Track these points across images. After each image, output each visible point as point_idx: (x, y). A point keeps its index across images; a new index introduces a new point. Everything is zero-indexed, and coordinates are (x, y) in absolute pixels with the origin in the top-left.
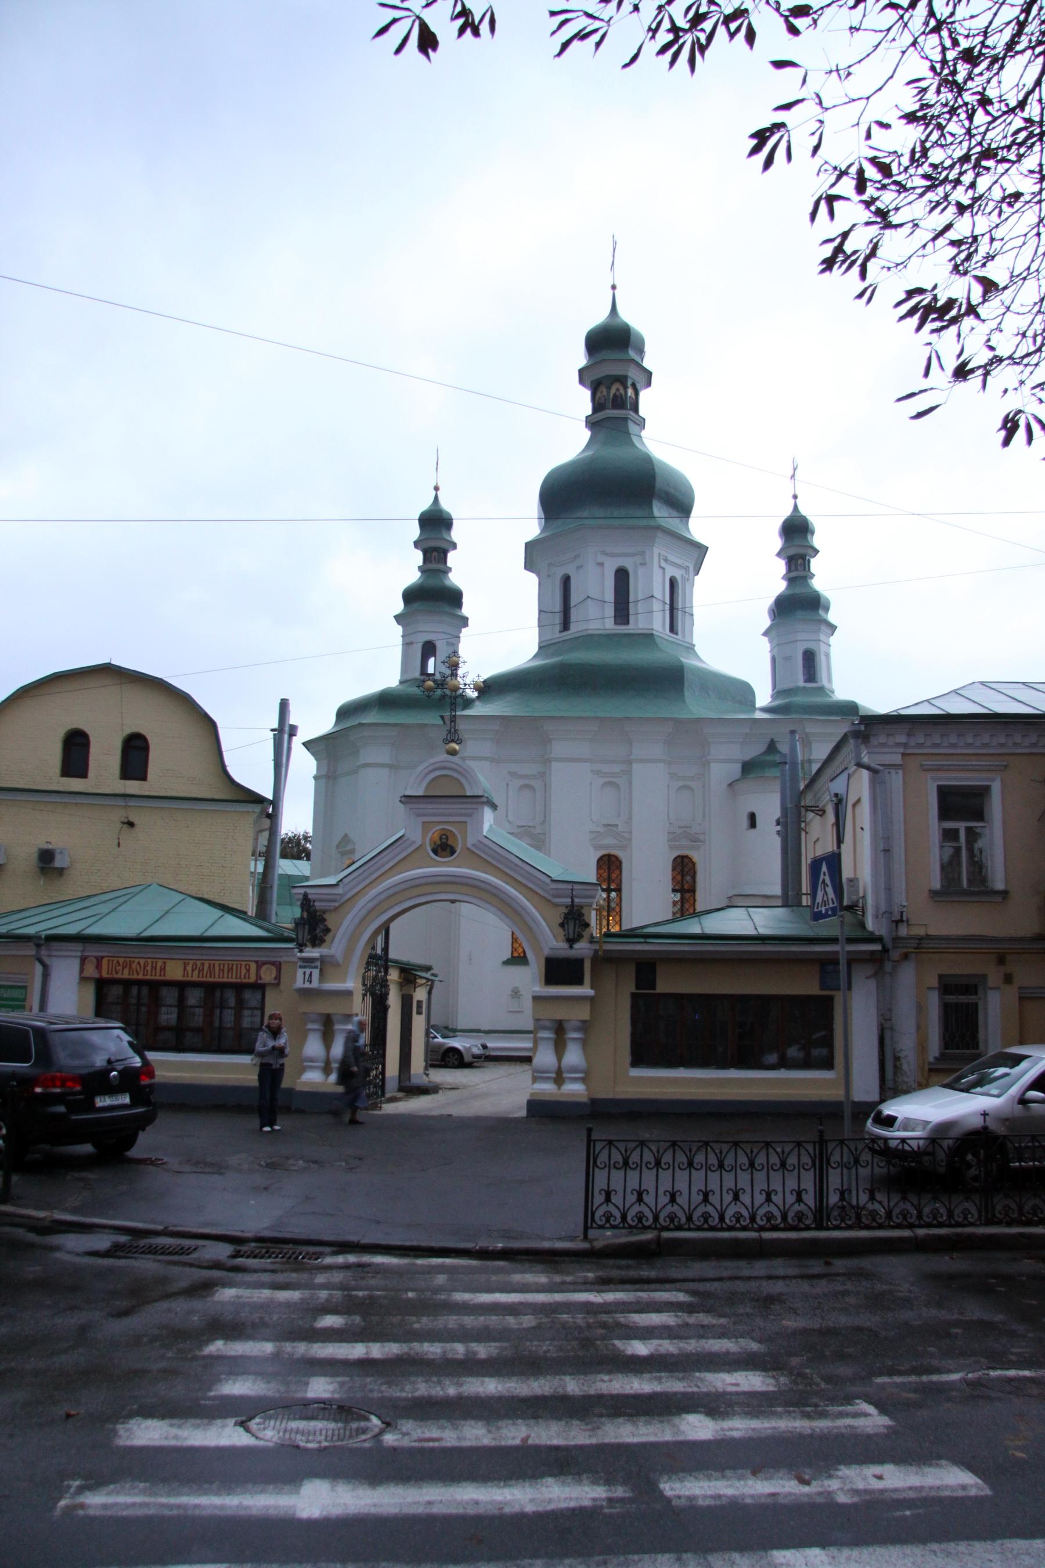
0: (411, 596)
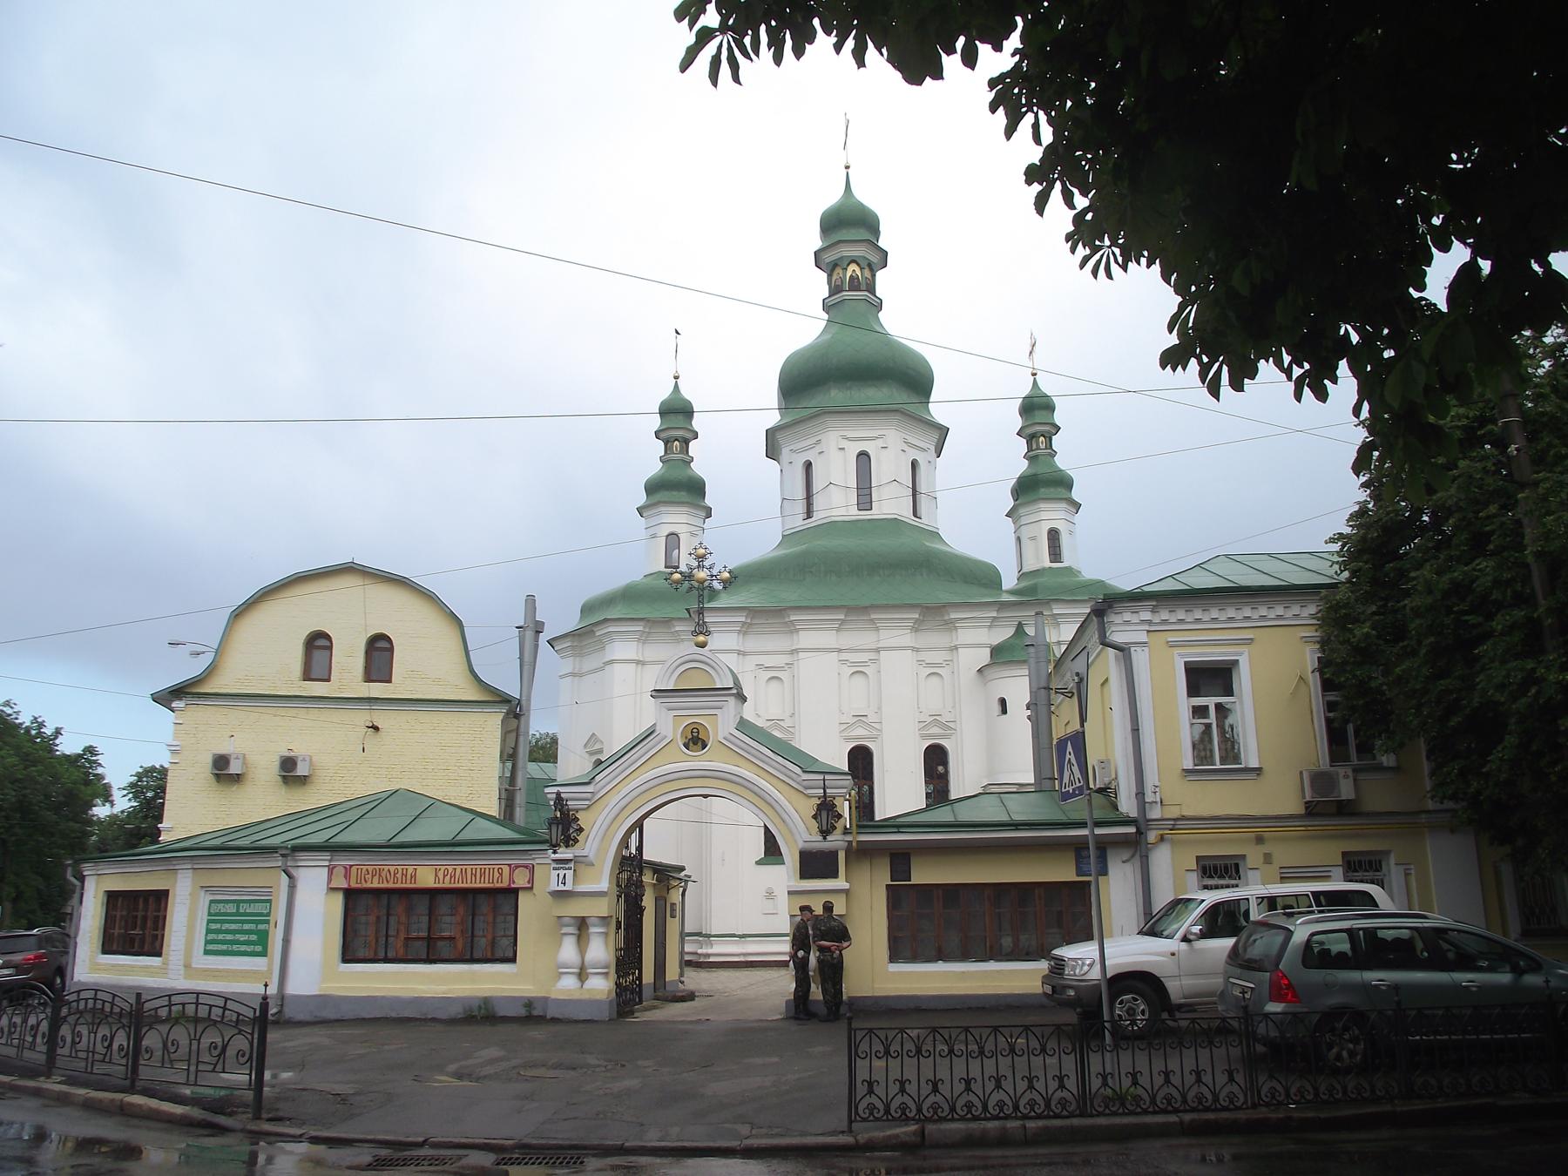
0: (653, 487)
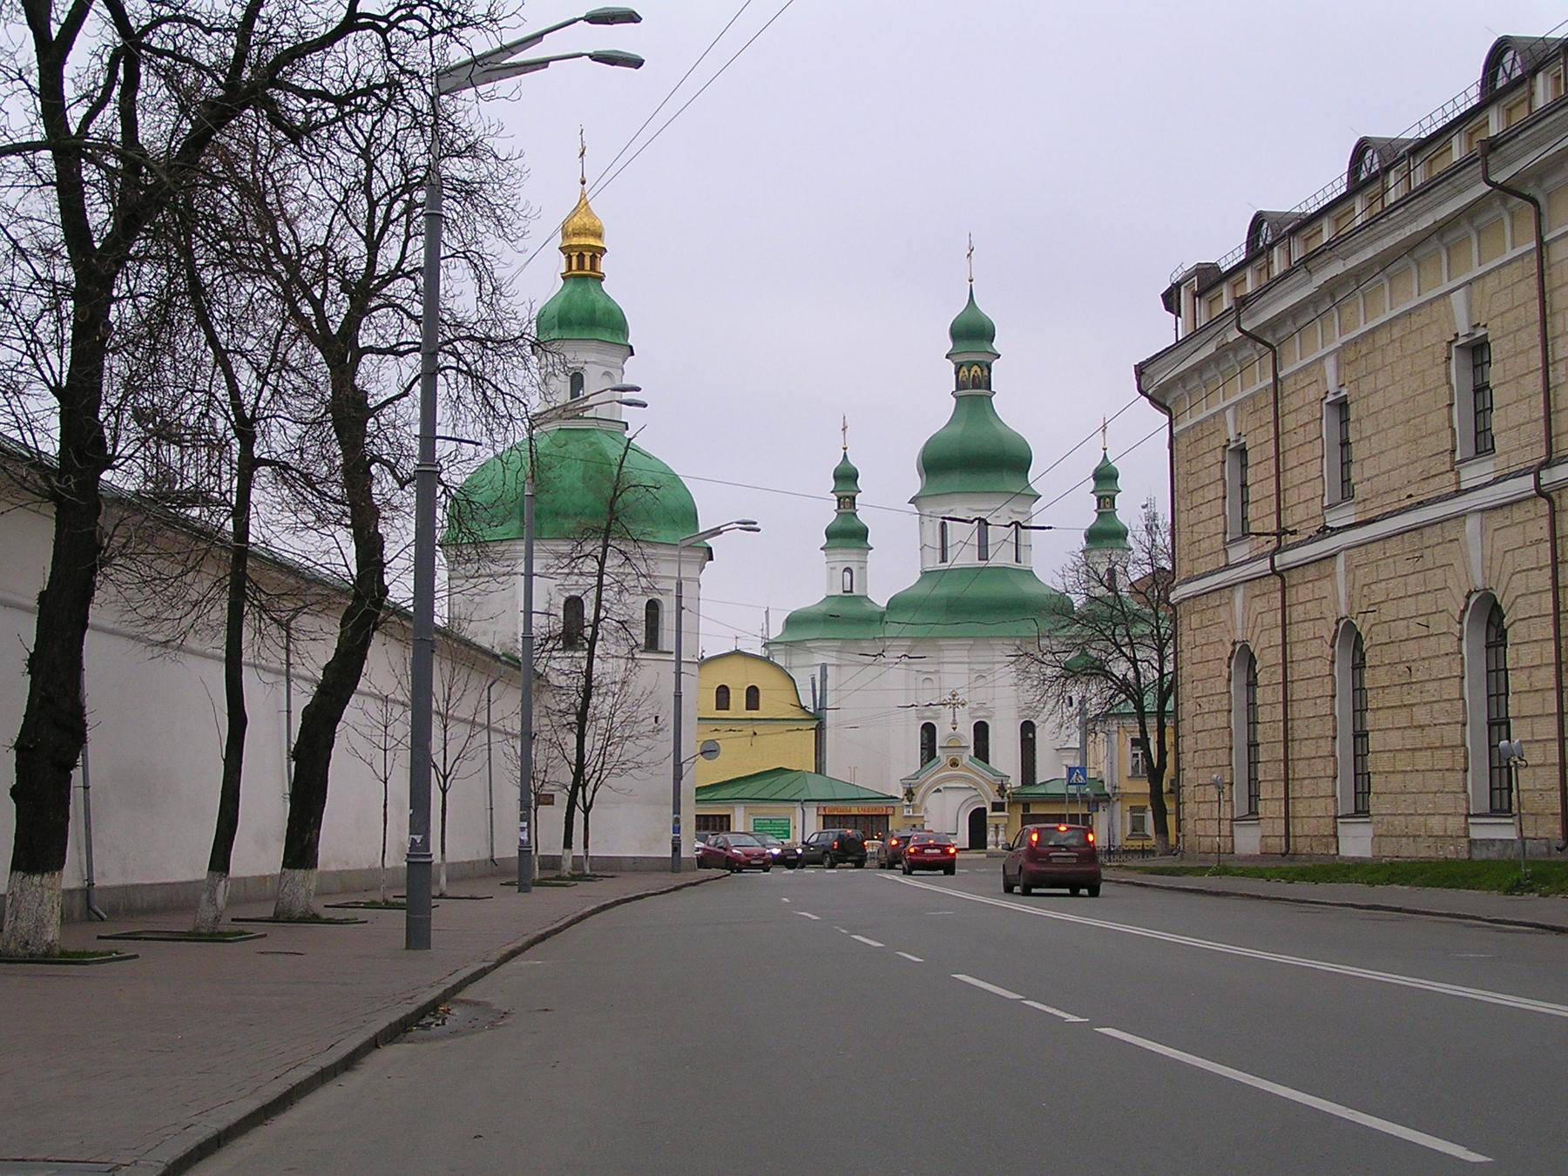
0: (830, 534)
